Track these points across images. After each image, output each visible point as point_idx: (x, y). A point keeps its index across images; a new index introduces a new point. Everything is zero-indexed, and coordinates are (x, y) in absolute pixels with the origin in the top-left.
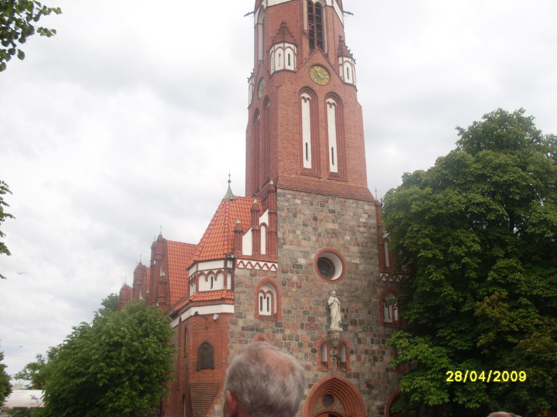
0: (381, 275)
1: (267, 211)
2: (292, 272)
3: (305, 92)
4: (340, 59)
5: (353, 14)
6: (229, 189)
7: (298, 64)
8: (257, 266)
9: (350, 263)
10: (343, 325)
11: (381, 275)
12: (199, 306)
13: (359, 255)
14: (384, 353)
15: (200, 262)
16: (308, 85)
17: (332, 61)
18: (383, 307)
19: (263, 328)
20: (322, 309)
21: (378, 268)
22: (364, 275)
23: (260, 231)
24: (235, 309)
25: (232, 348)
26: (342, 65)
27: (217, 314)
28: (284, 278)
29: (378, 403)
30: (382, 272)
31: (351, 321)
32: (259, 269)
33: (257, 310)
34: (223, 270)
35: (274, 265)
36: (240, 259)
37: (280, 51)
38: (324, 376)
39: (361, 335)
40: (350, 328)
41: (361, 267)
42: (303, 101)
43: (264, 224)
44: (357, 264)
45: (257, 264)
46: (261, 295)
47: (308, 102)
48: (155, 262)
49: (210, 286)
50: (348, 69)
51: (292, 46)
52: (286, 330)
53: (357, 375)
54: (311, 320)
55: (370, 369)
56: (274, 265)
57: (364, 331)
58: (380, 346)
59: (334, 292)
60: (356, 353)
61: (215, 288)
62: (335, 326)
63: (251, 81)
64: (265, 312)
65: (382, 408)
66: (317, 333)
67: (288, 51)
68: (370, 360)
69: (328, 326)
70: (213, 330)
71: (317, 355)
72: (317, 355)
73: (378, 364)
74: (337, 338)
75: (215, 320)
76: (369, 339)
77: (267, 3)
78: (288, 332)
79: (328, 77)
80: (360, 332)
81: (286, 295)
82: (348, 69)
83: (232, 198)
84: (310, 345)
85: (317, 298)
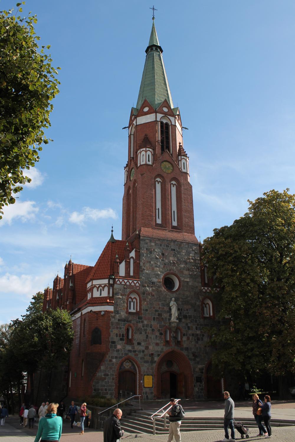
0: (202, 288)
1: (134, 250)
2: (148, 286)
3: (158, 177)
4: (180, 157)
5: (188, 129)
6: (112, 236)
7: (154, 161)
8: (128, 283)
9: (184, 281)
10: (178, 318)
11: (202, 288)
12: (93, 306)
13: (189, 276)
14: (203, 335)
15: (94, 279)
16: (159, 173)
17: (174, 158)
18: (203, 307)
19: (131, 320)
20: (166, 309)
21: (200, 284)
22: (192, 288)
23: (130, 262)
24: (114, 308)
25: (112, 332)
26: (181, 160)
27: (103, 311)
28: (144, 290)
29: (200, 366)
30: (203, 287)
31: (184, 317)
32: (129, 284)
33: (127, 309)
34: (108, 285)
35: (138, 282)
36: (118, 278)
37: (143, 153)
38: (166, 349)
39: (189, 325)
40: (183, 320)
41: (190, 284)
42: (157, 183)
43: (132, 257)
44: (188, 282)
45: (128, 281)
46: (130, 300)
47: (160, 183)
48: (67, 277)
49: (99, 295)
50: (184, 163)
51: (151, 150)
52: (144, 321)
53: (187, 349)
54: (160, 315)
55: (195, 346)
56: (138, 282)
57: (191, 322)
58: (201, 331)
59: (173, 299)
60: (187, 335)
61: (102, 296)
62: (174, 319)
63: (126, 169)
64: (132, 310)
65: (203, 369)
66: (163, 324)
67: (149, 153)
68: (195, 340)
69: (170, 319)
70: (101, 321)
71: (163, 336)
72: (163, 336)
73: (200, 342)
74: (175, 326)
75: (102, 315)
76: (194, 327)
77: (136, 123)
78: (146, 322)
79: (171, 168)
80: (189, 323)
81: (145, 300)
82: (184, 163)
83: (113, 241)
84: (159, 330)
85: (163, 302)
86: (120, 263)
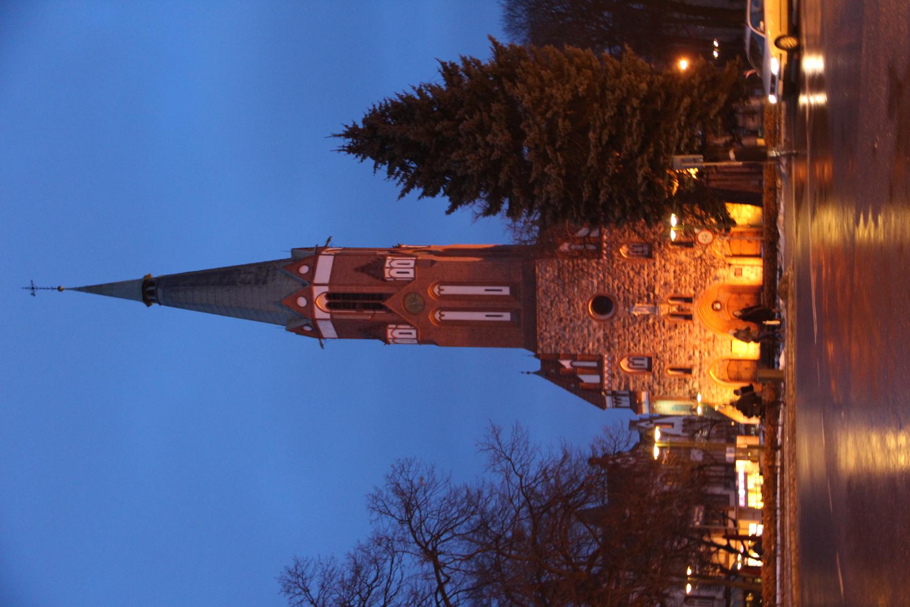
26: (395, 278)
42: (443, 318)
43: (571, 364)
51: (389, 331)
67: (396, 333)
79: (413, 295)
86: (582, 381)
